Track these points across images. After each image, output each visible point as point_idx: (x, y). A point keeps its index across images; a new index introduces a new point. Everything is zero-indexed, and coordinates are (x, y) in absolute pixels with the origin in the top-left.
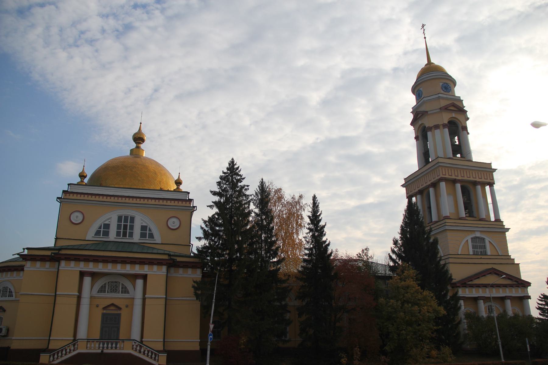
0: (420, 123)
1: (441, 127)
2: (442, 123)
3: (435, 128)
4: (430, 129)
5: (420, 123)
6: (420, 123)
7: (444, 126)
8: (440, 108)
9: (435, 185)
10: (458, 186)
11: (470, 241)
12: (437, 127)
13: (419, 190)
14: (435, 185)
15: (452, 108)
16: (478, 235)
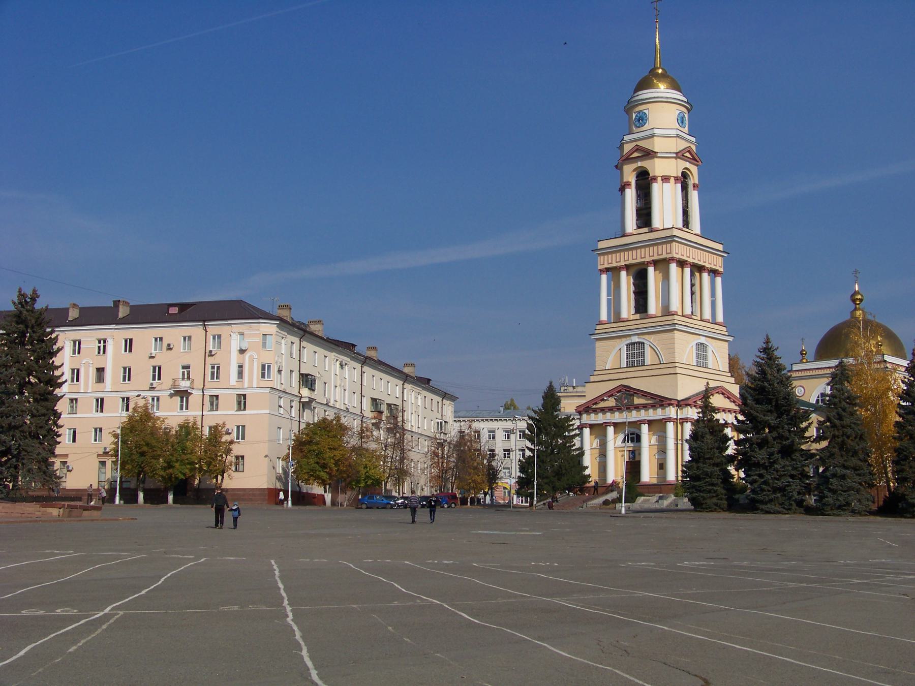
0: (639, 165)
1: (672, 180)
2: (675, 175)
3: (662, 180)
4: (655, 179)
5: (640, 164)
6: (640, 164)
7: (676, 179)
8: (677, 153)
9: (662, 264)
10: (687, 271)
11: (695, 347)
12: (666, 179)
13: (625, 265)
14: (662, 264)
15: (688, 155)
16: (702, 340)
